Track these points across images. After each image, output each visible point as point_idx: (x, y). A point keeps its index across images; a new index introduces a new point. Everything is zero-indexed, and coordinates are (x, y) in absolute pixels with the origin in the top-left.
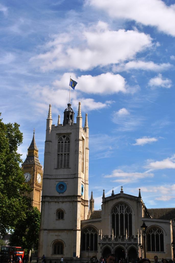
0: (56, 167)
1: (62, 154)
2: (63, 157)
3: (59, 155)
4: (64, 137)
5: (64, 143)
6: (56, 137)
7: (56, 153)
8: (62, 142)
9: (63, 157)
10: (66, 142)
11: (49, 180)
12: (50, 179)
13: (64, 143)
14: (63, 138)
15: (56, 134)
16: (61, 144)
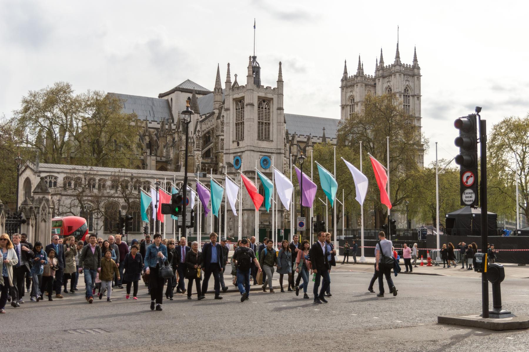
0: (235, 139)
1: (239, 123)
2: (240, 126)
3: (236, 124)
4: (240, 102)
5: (240, 109)
6: (233, 103)
7: (235, 122)
8: (239, 109)
9: (240, 126)
10: (242, 108)
11: (228, 155)
12: (229, 154)
13: (240, 109)
14: (239, 104)
15: (234, 99)
16: (238, 111)
